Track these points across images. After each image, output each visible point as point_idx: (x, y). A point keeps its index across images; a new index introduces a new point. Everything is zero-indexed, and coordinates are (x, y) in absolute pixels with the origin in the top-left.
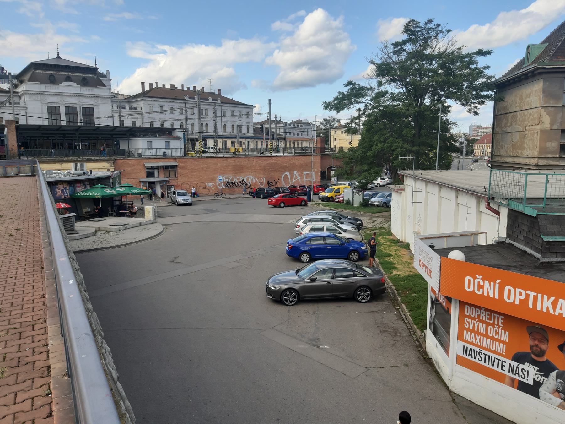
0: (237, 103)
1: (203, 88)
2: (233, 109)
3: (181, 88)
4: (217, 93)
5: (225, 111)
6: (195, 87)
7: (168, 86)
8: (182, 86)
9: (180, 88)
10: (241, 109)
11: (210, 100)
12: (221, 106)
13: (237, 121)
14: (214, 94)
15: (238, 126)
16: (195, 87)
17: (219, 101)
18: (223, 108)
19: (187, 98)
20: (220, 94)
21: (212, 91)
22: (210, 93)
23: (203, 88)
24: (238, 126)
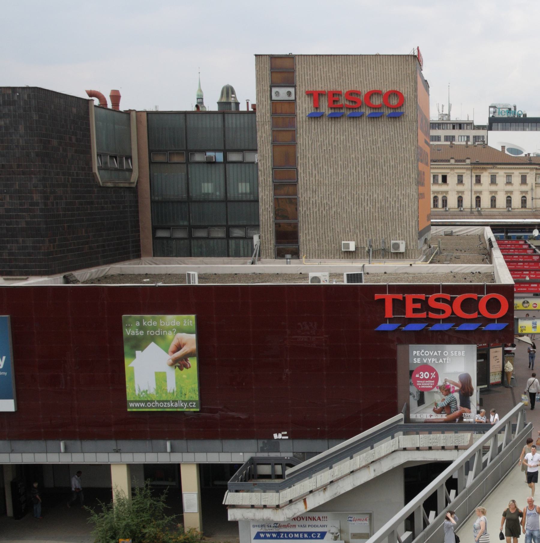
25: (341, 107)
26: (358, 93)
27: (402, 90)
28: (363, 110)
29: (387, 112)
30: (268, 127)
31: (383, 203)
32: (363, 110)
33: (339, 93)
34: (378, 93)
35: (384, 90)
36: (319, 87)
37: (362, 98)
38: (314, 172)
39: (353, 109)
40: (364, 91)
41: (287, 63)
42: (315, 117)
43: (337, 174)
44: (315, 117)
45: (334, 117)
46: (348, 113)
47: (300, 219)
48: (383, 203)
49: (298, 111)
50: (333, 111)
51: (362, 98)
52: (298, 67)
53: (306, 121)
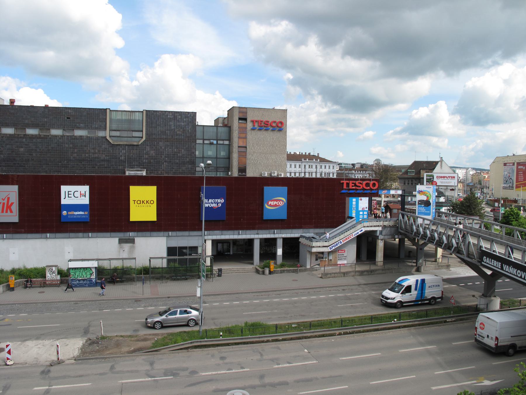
0: (326, 161)
1: (310, 153)
2: (325, 164)
3: (299, 154)
4: (317, 155)
5: (321, 166)
6: (306, 153)
7: (292, 153)
8: (300, 152)
9: (298, 153)
10: (330, 165)
11: (314, 160)
12: (319, 163)
13: (327, 170)
14: (315, 156)
15: (328, 173)
16: (306, 153)
17: (319, 161)
18: (320, 164)
19: (303, 160)
20: (318, 156)
21: (315, 154)
22: (313, 155)
23: (310, 153)
24: (328, 173)
25: (262, 126)
26: (268, 122)
27: (283, 121)
28: (270, 127)
29: (278, 129)
30: (237, 132)
31: (276, 160)
32: (270, 127)
33: (262, 121)
34: (275, 122)
35: (277, 121)
36: (255, 119)
37: (270, 123)
38: (252, 148)
39: (266, 127)
40: (270, 121)
41: (244, 110)
42: (253, 129)
43: (260, 149)
44: (253, 129)
45: (260, 130)
46: (265, 128)
47: (247, 165)
48: (276, 160)
49: (248, 127)
50: (260, 127)
51: (270, 123)
52: (248, 112)
53: (250, 130)
